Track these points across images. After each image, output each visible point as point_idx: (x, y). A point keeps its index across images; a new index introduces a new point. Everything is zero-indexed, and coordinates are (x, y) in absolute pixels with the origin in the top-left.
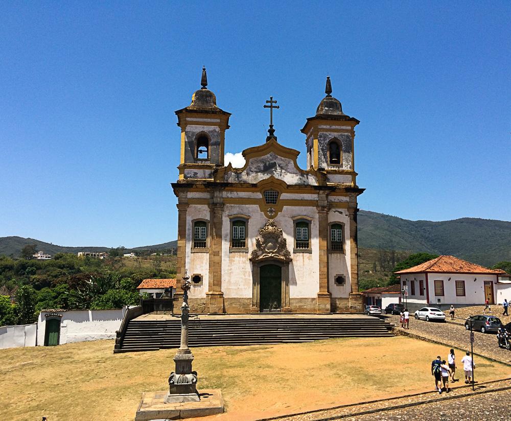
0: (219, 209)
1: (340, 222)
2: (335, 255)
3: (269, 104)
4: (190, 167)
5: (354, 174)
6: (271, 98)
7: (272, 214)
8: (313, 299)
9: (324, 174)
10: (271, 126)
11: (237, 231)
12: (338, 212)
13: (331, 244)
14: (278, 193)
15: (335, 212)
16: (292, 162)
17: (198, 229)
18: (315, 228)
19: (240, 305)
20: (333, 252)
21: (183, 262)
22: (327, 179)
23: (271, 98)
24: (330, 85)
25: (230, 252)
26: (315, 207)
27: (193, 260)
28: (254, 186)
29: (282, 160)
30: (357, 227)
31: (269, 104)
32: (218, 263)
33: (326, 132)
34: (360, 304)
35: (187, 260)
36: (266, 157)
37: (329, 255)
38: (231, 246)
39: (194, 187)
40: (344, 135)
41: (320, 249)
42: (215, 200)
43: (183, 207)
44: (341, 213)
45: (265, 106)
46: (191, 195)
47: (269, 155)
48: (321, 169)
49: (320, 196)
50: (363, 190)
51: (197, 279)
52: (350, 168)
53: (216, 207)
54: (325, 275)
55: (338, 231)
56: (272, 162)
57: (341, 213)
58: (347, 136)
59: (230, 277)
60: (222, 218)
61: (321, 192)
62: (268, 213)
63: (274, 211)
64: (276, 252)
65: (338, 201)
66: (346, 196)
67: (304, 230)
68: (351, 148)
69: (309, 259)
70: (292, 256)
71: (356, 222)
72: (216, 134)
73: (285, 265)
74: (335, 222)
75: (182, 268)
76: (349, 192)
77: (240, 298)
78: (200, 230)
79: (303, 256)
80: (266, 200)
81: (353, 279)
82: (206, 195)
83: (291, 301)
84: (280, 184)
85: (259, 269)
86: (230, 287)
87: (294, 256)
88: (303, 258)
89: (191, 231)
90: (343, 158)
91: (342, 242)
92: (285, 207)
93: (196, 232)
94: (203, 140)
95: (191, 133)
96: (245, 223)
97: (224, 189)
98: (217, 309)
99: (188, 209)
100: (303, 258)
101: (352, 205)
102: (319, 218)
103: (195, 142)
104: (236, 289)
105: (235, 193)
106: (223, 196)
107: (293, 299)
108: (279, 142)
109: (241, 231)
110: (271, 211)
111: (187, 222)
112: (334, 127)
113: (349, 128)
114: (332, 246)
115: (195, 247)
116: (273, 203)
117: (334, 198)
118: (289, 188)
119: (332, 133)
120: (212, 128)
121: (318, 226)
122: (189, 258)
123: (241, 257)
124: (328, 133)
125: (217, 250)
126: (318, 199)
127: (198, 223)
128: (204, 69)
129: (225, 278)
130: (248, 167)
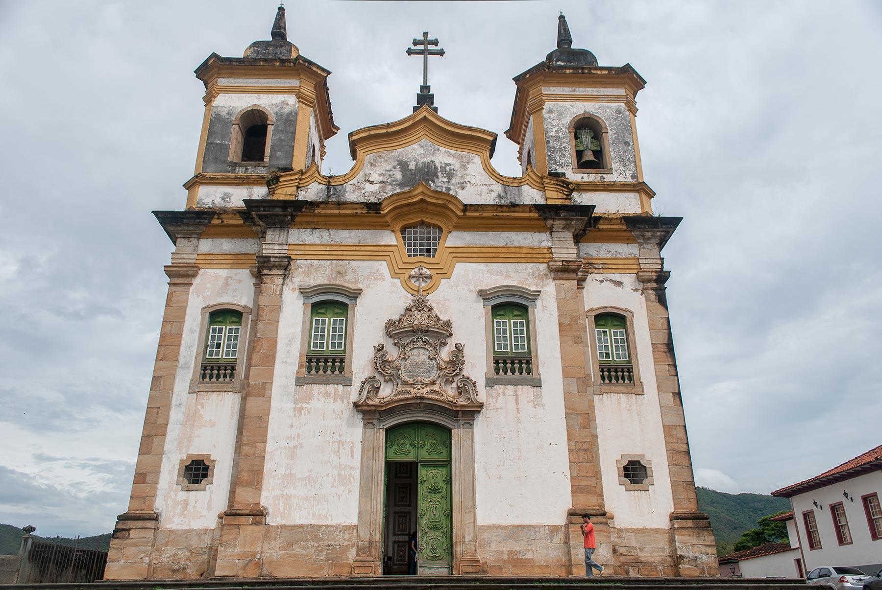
0: (275, 272)
1: (622, 310)
2: (614, 397)
3: (422, 47)
4: (213, 181)
5: (642, 189)
6: (426, 34)
7: (423, 284)
8: (554, 529)
9: (564, 182)
10: (425, 88)
11: (323, 330)
12: (611, 281)
13: (598, 369)
14: (441, 230)
15: (602, 281)
16: (477, 160)
17: (220, 331)
18: (546, 318)
19: (319, 551)
20: (604, 388)
21: (160, 421)
22: (568, 197)
23: (426, 34)
24: (566, 30)
25: (300, 382)
26: (545, 265)
27: (192, 418)
28: (373, 208)
29: (450, 155)
30: (668, 319)
31: (422, 47)
32: (260, 418)
33: (564, 100)
34: (709, 550)
35: (175, 415)
36: (409, 149)
37: (596, 398)
38: (304, 370)
39: (215, 222)
40: (610, 108)
41: (566, 374)
42: (266, 252)
43: (180, 275)
44: (619, 284)
45: (410, 52)
46: (206, 245)
47: (416, 146)
48: (556, 176)
49: (555, 235)
50: (674, 222)
51: (197, 471)
52: (633, 177)
53: (263, 268)
54: (585, 450)
55: (615, 334)
56: (425, 160)
57: (619, 284)
58: (619, 112)
59: (292, 457)
60: (281, 294)
61: (557, 222)
62: (413, 280)
63: (429, 277)
64: (433, 383)
65: (609, 256)
66: (628, 241)
67: (515, 323)
68: (631, 133)
69: (537, 402)
70: (482, 394)
71: (666, 307)
72: (287, 110)
73: (462, 422)
74: (606, 307)
75: (156, 439)
76: (634, 227)
77: (320, 526)
78: (225, 334)
79: (516, 396)
80: (409, 251)
81: (675, 469)
82: (248, 246)
83: (485, 536)
84: (444, 206)
85: (382, 435)
86: (291, 491)
87: (489, 395)
88: (517, 404)
89: (196, 335)
90: (612, 155)
91: (630, 361)
92: (461, 269)
93: (213, 338)
94: (254, 127)
95: (226, 110)
96: (346, 306)
97: (293, 217)
98: (240, 563)
99: (196, 281)
100: (517, 404)
101: (650, 265)
102: (558, 291)
103: (235, 129)
104: (306, 499)
105: (325, 233)
106: (290, 241)
107: (490, 527)
108: (439, 114)
109: (334, 329)
110: (420, 277)
111: (189, 311)
112: (581, 91)
113: (621, 92)
114: (602, 371)
115: (204, 376)
116: (429, 256)
117: (596, 250)
118: (468, 214)
119: (579, 104)
120: (278, 98)
121: (556, 314)
122: (183, 409)
123: (331, 400)
124: (567, 104)
125: (260, 381)
126: (550, 245)
127: (221, 315)
128: (281, 9)
129: (275, 462)
130: (361, 173)
